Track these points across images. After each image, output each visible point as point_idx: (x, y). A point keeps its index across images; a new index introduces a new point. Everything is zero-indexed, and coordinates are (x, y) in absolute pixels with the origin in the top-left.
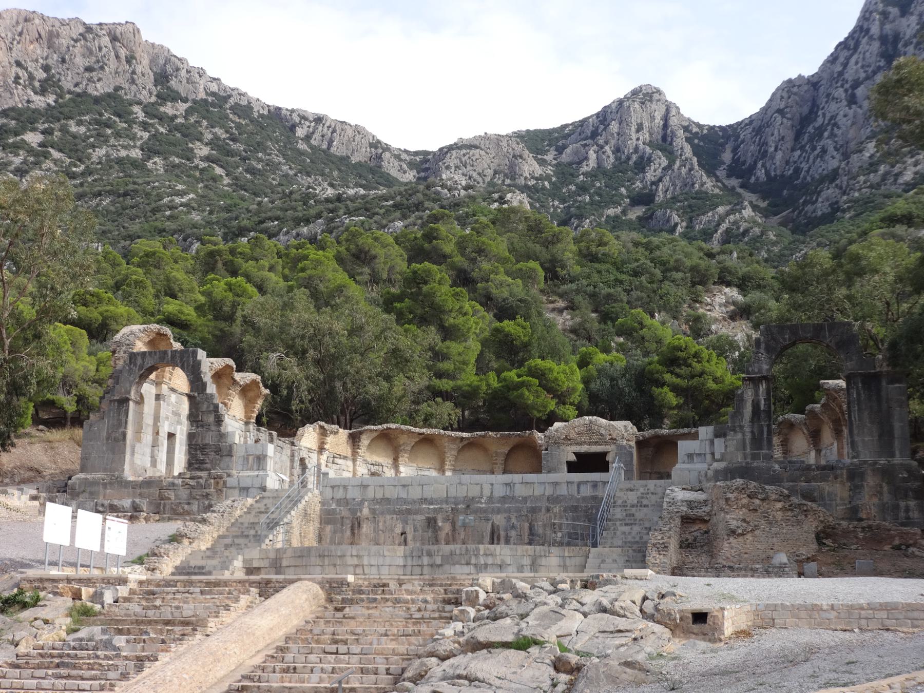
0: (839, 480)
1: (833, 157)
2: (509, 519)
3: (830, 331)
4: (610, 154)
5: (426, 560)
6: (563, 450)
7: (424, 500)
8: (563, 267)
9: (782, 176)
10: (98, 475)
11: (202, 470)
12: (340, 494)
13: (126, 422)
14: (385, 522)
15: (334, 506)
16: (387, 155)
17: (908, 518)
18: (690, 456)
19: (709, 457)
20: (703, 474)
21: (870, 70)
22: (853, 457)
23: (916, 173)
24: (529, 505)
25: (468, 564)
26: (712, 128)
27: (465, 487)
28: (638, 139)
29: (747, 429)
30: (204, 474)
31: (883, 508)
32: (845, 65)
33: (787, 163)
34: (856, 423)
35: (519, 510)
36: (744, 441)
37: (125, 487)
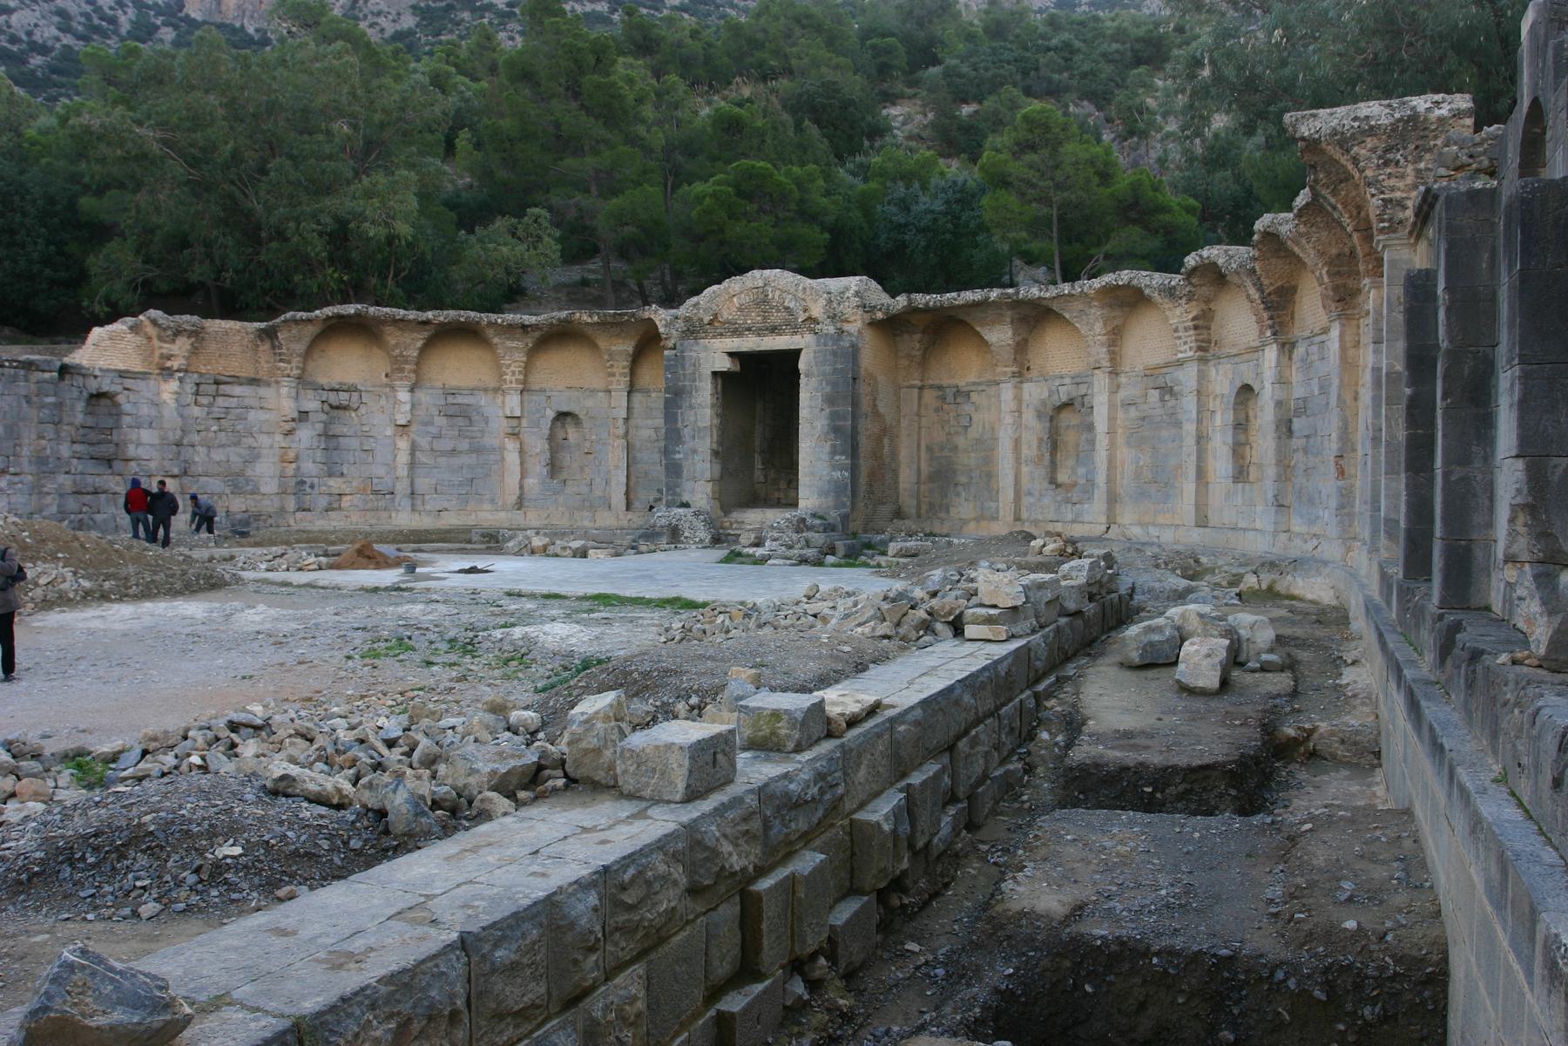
6: (706, 348)
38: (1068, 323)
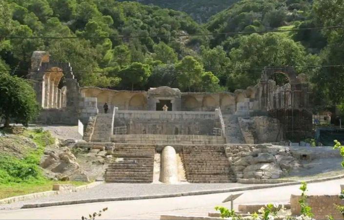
2: (181, 126)
5: (175, 139)
7: (152, 119)
12: (121, 116)
15: (120, 120)
18: (242, 107)
19: (247, 108)
25: (189, 141)
29: (260, 99)
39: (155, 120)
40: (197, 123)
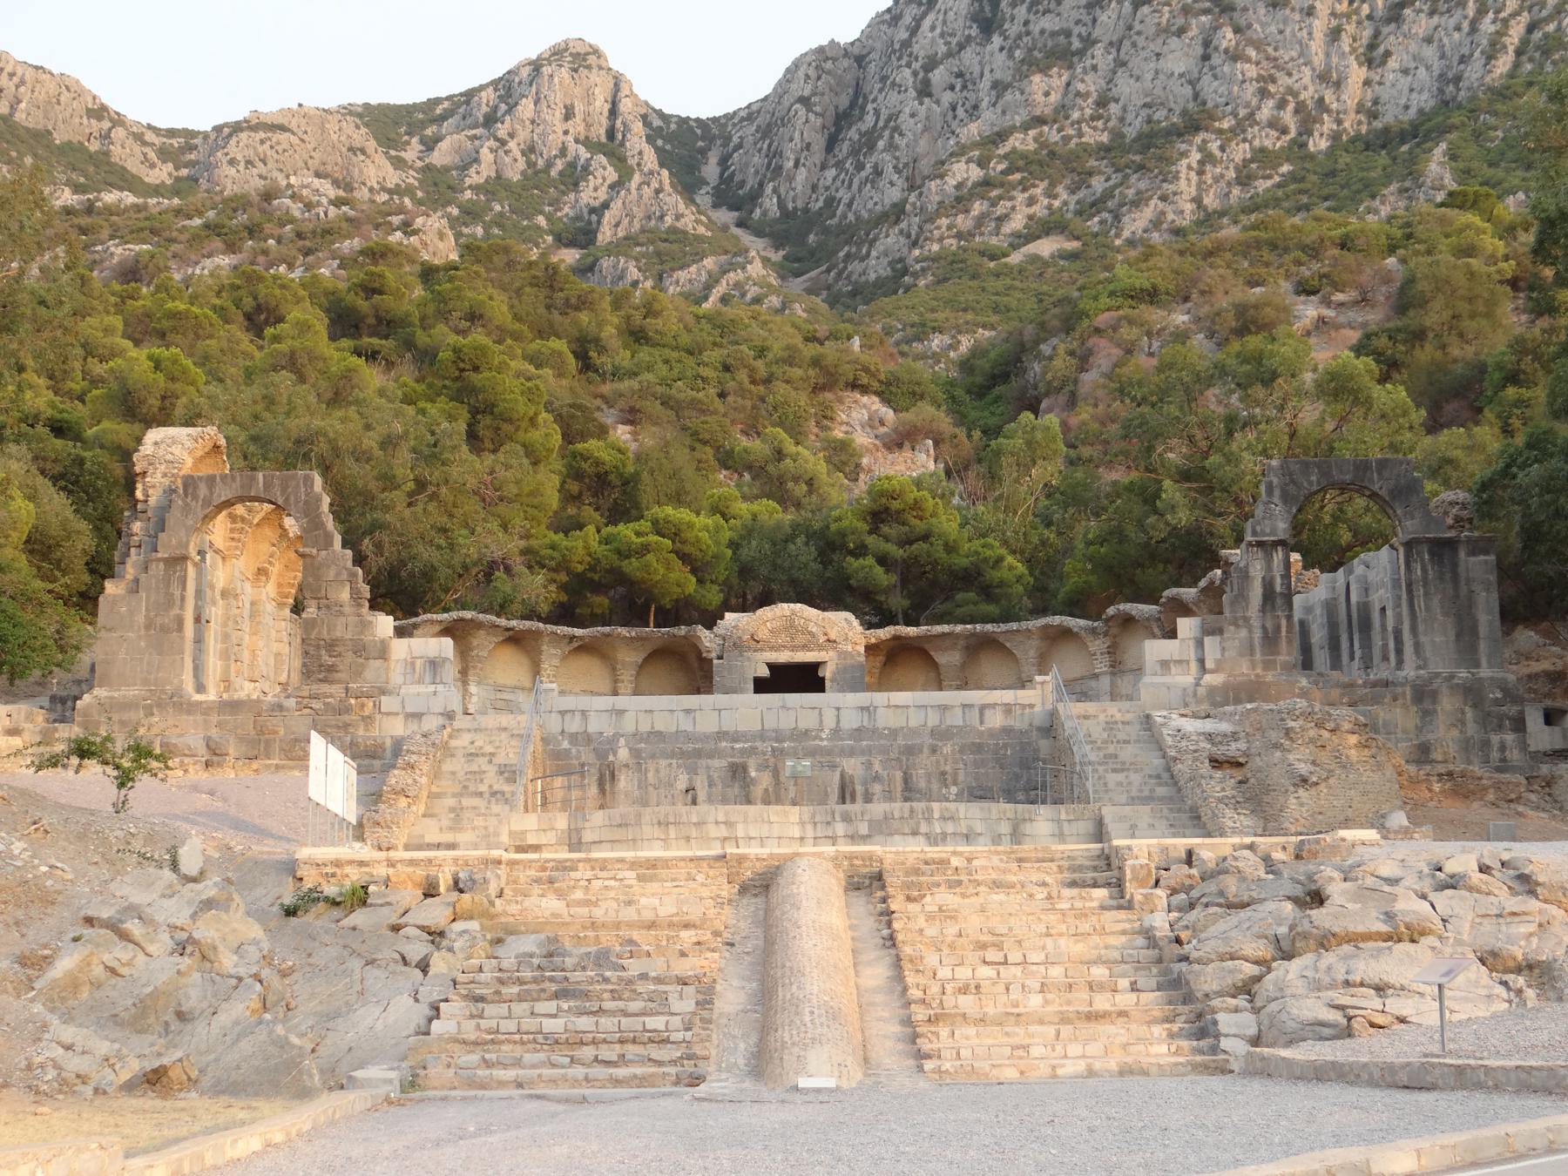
0: (1400, 701)
1: (892, 184)
2: (869, 765)
3: (1379, 474)
4: (519, 156)
6: (749, 659)
7: (721, 735)
8: (602, 349)
9: (806, 210)
10: (133, 692)
11: (331, 682)
12: (574, 725)
13: (183, 599)
14: (657, 771)
15: (565, 745)
16: (118, 133)
17: (1504, 760)
18: (1165, 665)
19: (1194, 666)
20: (1190, 691)
21: (954, 41)
22: (1419, 668)
23: (1031, 218)
24: (901, 741)
25: (915, 833)
26: (684, 121)
27: (792, 713)
28: (566, 133)
29: (1256, 624)
30: (337, 690)
31: (1466, 746)
32: (914, 31)
33: (814, 188)
34: (1421, 614)
35: (885, 751)
36: (1251, 639)
37: (189, 712)
38: (1010, 653)
39: (735, 737)
40: (947, 749)
